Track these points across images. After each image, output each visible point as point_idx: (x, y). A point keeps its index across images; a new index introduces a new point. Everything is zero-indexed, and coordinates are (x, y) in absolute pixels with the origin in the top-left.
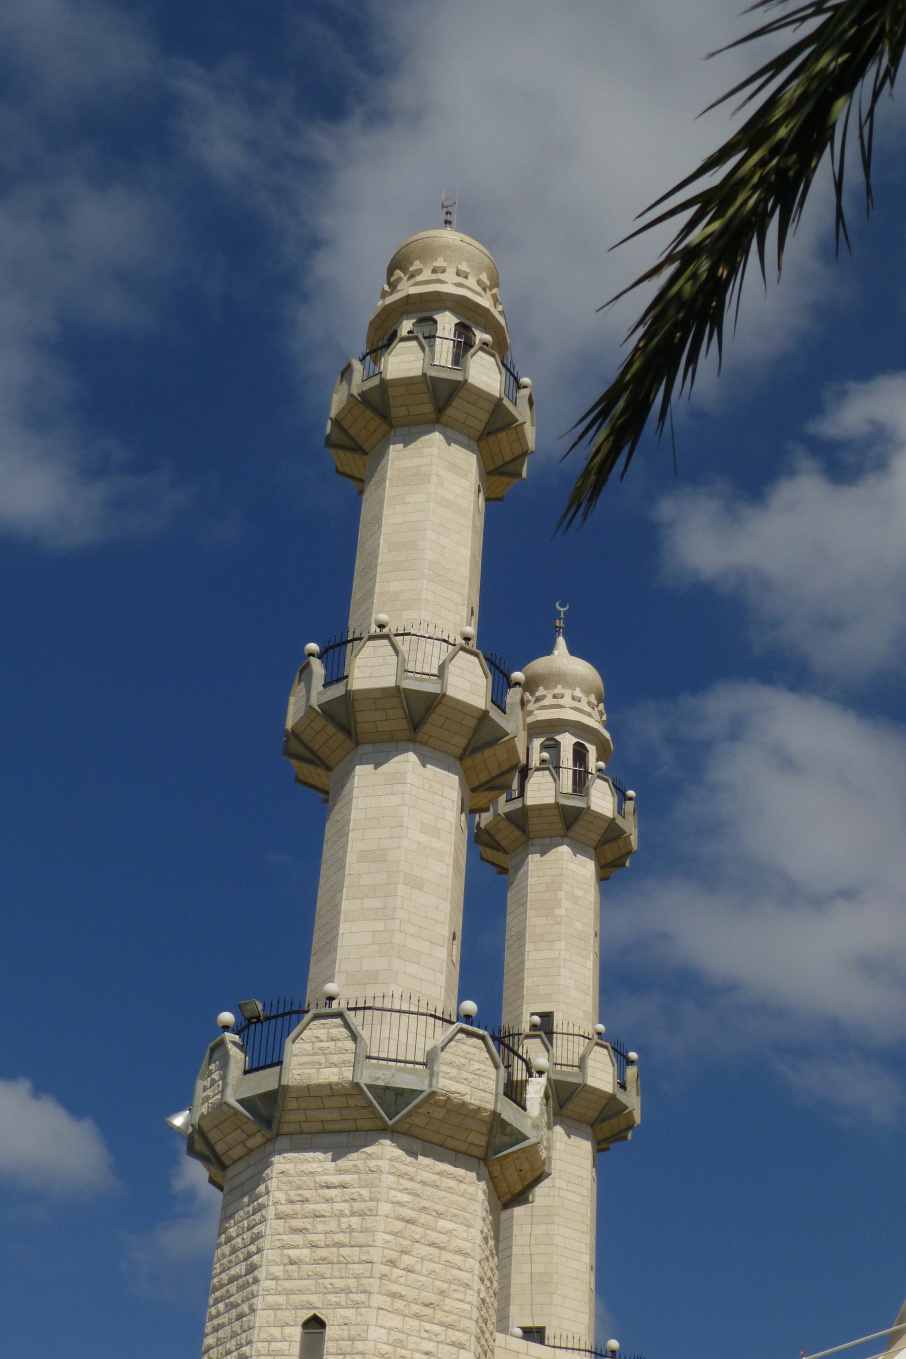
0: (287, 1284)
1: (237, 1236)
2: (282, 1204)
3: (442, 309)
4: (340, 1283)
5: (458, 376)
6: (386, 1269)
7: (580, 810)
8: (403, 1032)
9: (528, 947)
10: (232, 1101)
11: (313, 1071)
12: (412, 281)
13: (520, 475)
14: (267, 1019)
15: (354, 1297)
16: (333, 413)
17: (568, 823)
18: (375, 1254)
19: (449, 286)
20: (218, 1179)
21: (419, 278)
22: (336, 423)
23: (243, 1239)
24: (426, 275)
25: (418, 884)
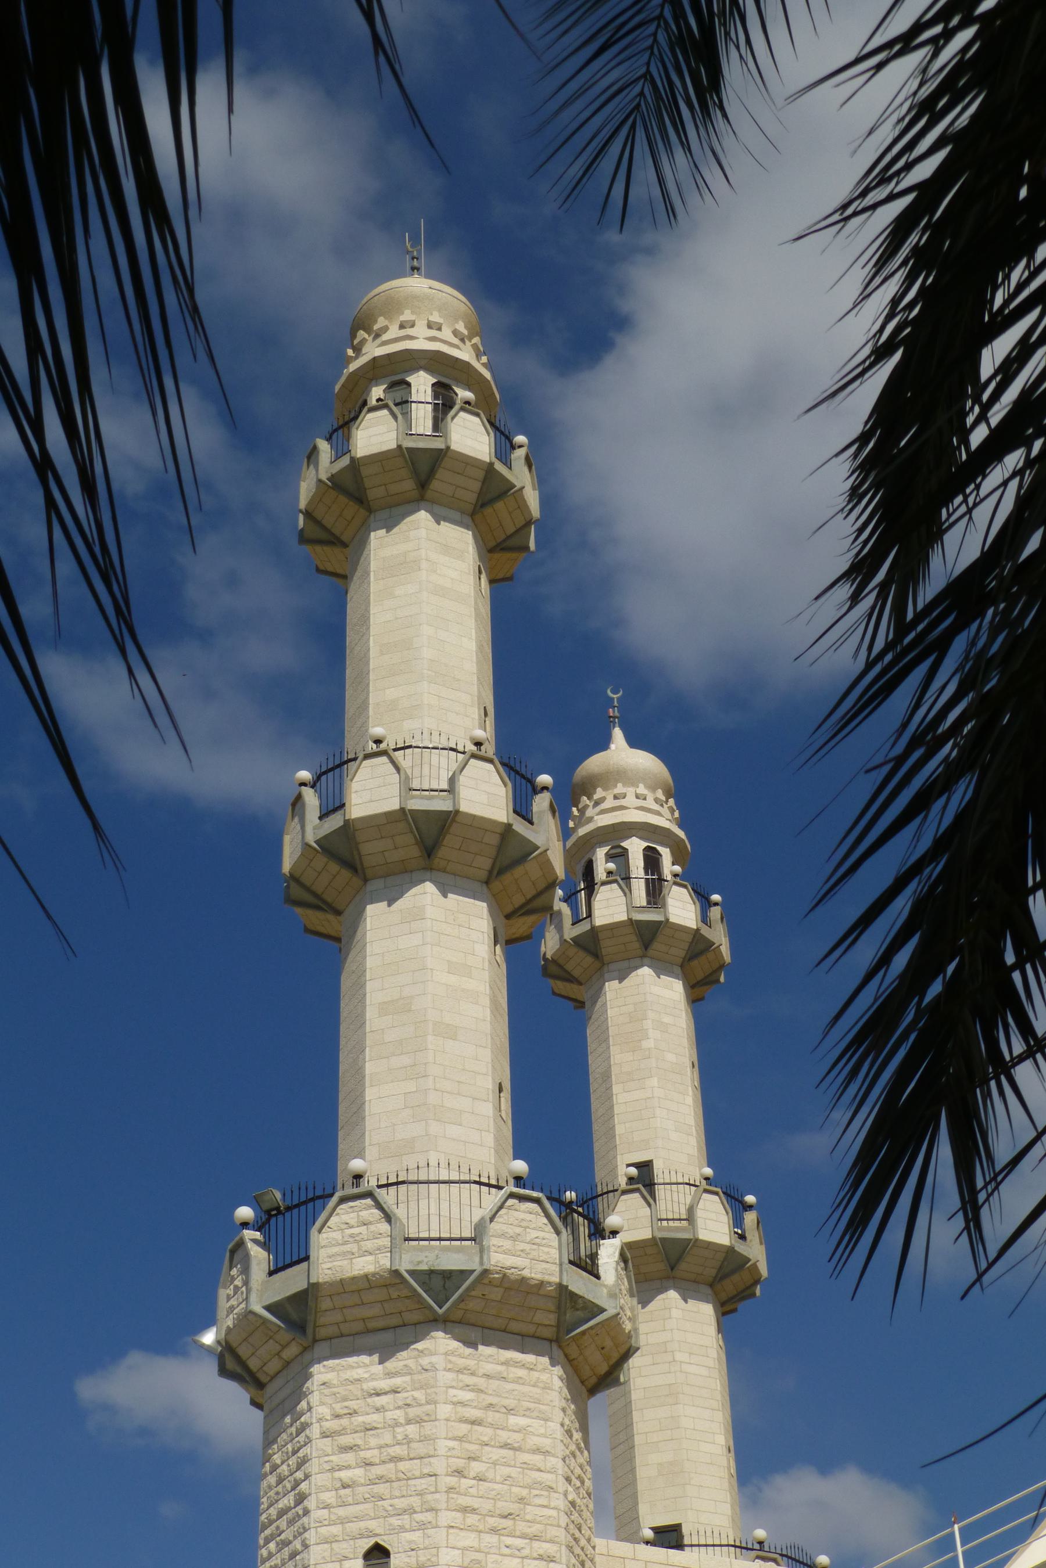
0: (341, 1512)
1: (283, 1463)
2: (327, 1420)
4: (401, 1504)
5: (438, 444)
6: (452, 1481)
7: (660, 922)
8: (445, 1205)
9: (616, 1089)
10: (258, 1309)
11: (346, 1262)
12: (378, 341)
13: (527, 548)
14: (289, 1209)
15: (418, 1517)
16: (303, 504)
17: (646, 940)
18: (439, 1465)
19: (421, 342)
20: (260, 1400)
21: (385, 337)
22: (308, 514)
23: (289, 1465)
24: (394, 332)
25: (451, 1033)
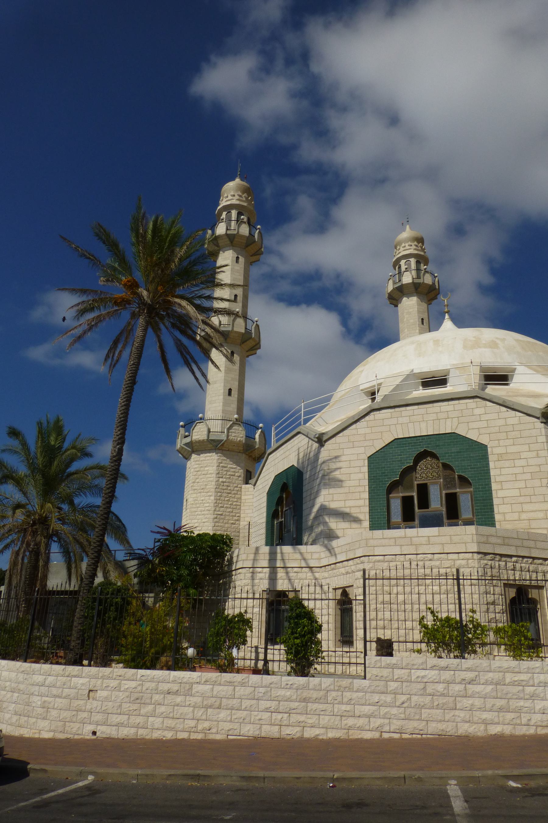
25: (215, 382)
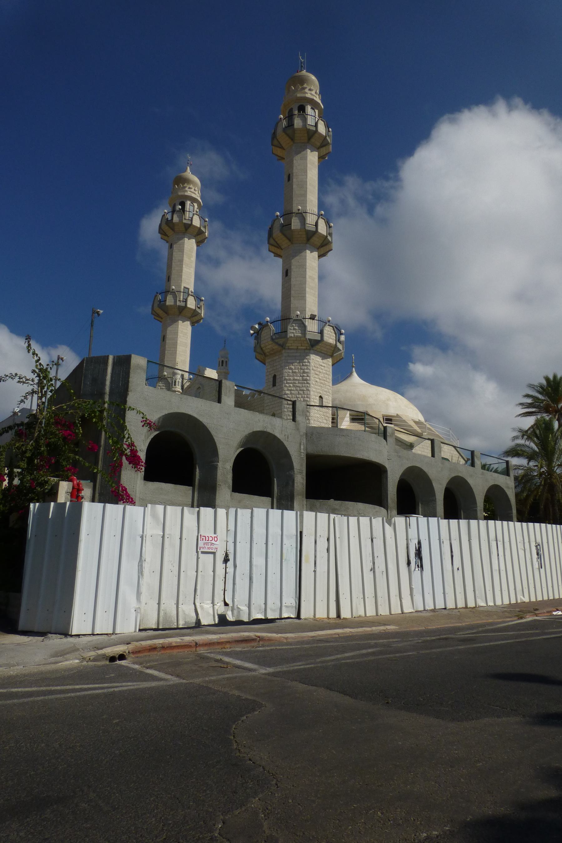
3: (317, 109)
4: (325, 390)
9: (184, 266)
